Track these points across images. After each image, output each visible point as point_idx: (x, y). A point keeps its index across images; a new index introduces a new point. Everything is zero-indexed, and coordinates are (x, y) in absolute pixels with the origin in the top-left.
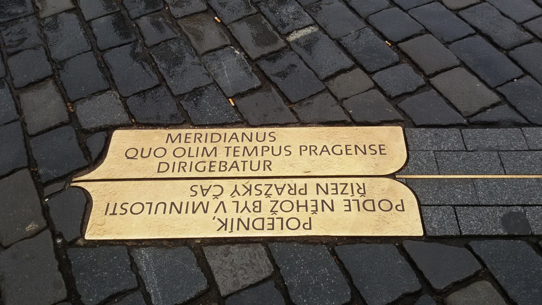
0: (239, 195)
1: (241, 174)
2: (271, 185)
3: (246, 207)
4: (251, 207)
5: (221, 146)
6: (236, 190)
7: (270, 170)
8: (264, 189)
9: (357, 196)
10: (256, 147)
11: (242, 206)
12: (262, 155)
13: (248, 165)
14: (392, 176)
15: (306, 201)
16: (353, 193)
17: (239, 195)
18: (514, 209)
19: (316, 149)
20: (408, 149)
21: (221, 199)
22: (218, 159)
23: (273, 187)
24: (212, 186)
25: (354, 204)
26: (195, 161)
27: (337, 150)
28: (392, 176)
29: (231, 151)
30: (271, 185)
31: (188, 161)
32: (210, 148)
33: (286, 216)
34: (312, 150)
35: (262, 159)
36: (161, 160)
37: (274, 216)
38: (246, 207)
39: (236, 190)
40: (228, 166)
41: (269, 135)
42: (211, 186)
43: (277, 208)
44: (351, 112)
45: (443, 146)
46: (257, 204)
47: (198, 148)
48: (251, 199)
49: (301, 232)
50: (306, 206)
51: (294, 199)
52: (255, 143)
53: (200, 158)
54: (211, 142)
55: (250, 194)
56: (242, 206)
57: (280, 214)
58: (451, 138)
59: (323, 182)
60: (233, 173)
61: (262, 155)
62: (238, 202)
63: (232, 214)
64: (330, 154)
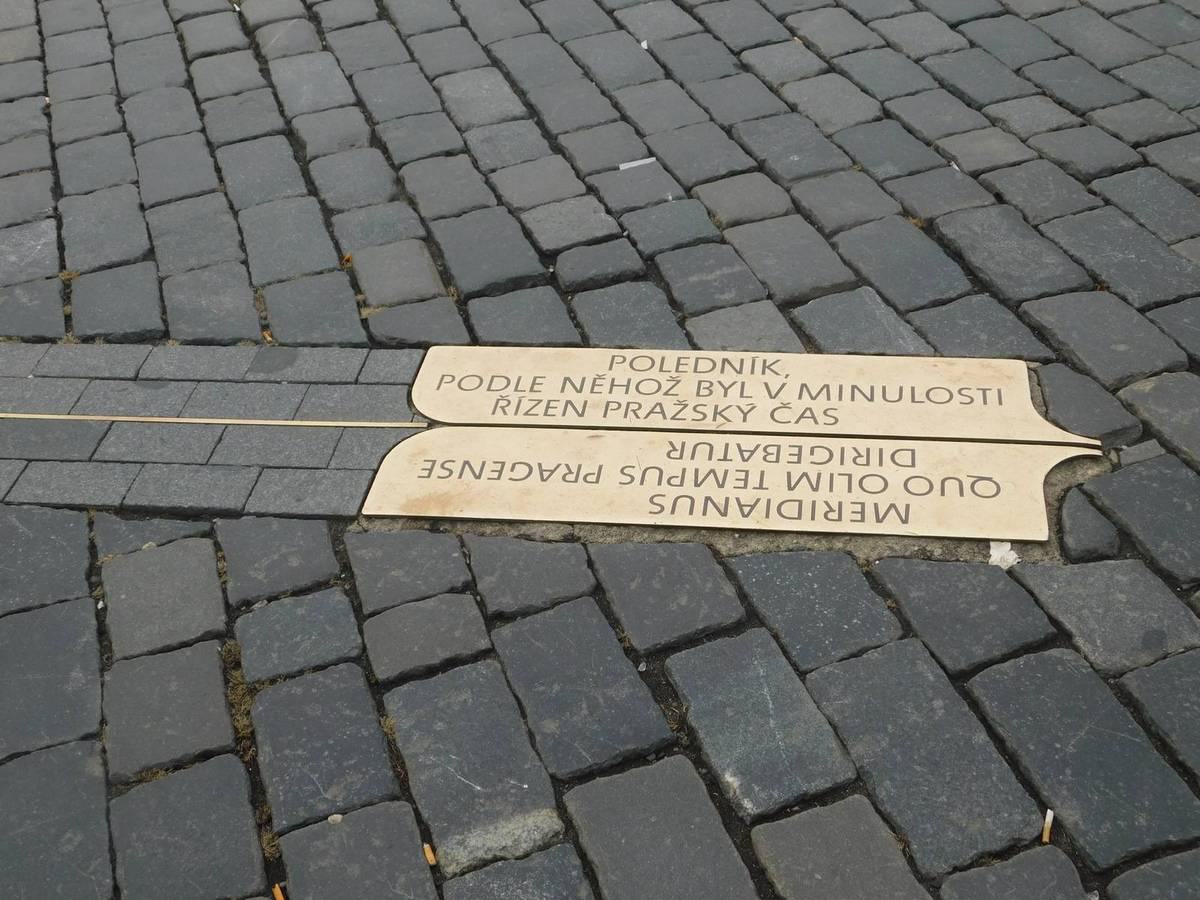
0: (739, 407)
1: (733, 439)
2: (673, 418)
3: (726, 390)
4: (716, 386)
5: (777, 491)
6: (745, 415)
7: (671, 443)
8: (688, 413)
9: (514, 398)
10: (697, 485)
11: (735, 391)
12: (684, 470)
13: (719, 453)
14: (433, 424)
15: (610, 392)
16: (520, 401)
17: (739, 407)
18: (261, 376)
19: (565, 475)
20: (376, 472)
21: (776, 403)
22: (783, 467)
23: (669, 415)
24: (793, 421)
25: (526, 384)
26: (834, 466)
27: (522, 471)
28: (433, 424)
29: (754, 480)
30: (673, 418)
31: (849, 467)
32: (803, 492)
33: (654, 373)
34: (573, 475)
35: (686, 462)
36: (911, 472)
37: (675, 375)
38: (726, 390)
39: (745, 415)
40: (760, 453)
41: (663, 508)
42: (797, 422)
43: (666, 386)
44: (456, 555)
45: (303, 477)
46: (704, 392)
47: (831, 490)
48: (718, 398)
49: (629, 354)
50: (612, 385)
51: (633, 395)
52: (699, 495)
53: (826, 471)
54: (800, 502)
55: (716, 407)
56: (735, 391)
57: (663, 378)
58: (274, 495)
59: (572, 418)
60: (748, 442)
61: (684, 470)
62: (742, 395)
63: (755, 385)
64: (540, 465)
